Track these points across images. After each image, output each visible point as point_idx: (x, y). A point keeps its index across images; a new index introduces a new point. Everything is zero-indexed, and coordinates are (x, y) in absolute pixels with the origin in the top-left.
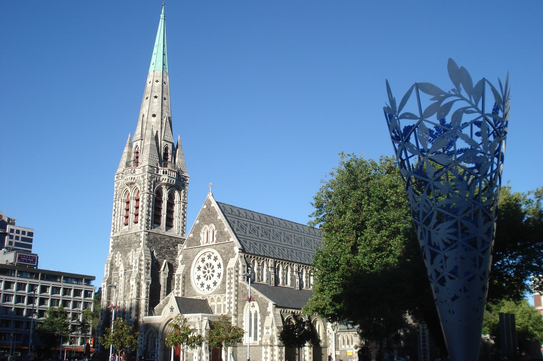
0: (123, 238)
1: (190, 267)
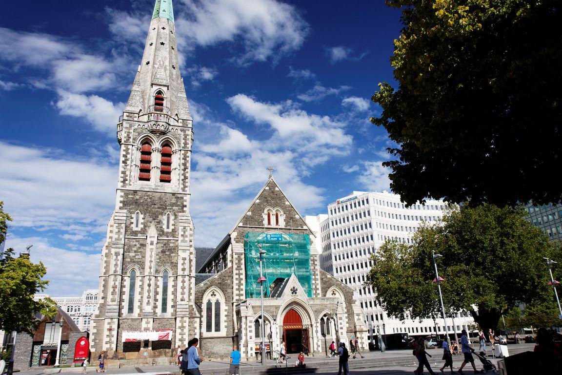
0: (148, 196)
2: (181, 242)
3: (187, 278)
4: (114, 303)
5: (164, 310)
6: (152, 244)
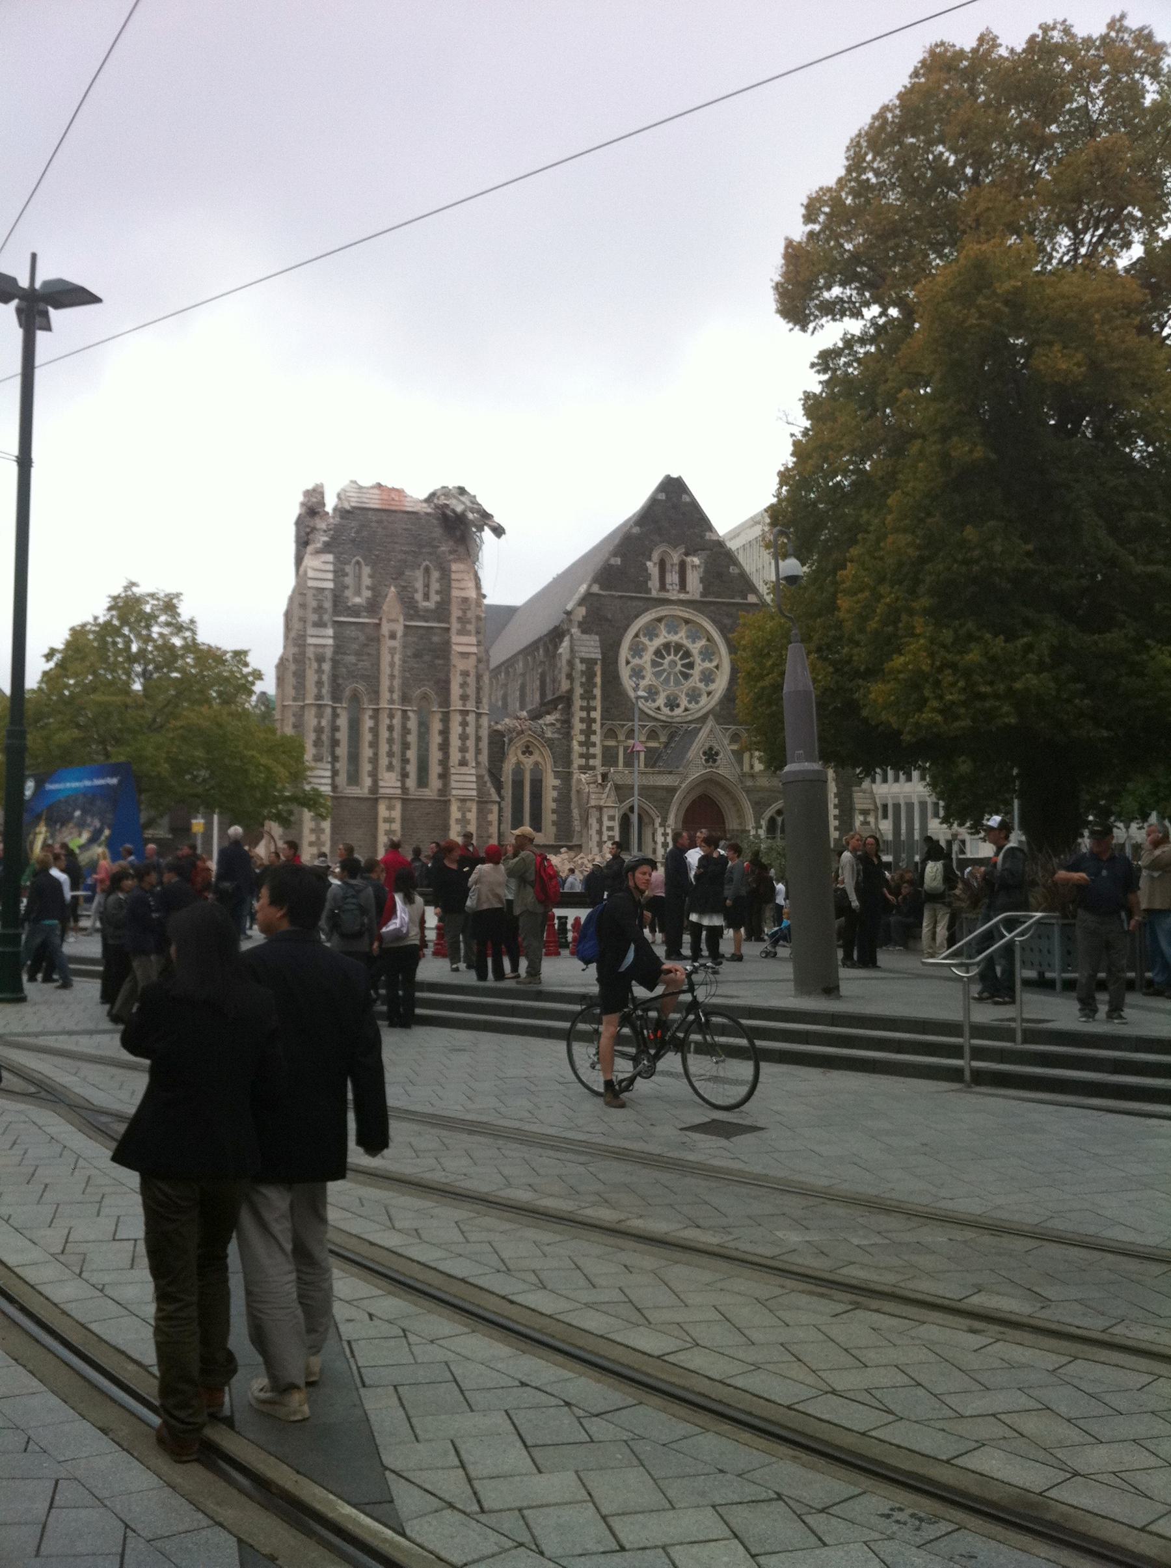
1: (618, 644)
3: (471, 718)
4: (319, 765)
5: (422, 782)
6: (393, 636)
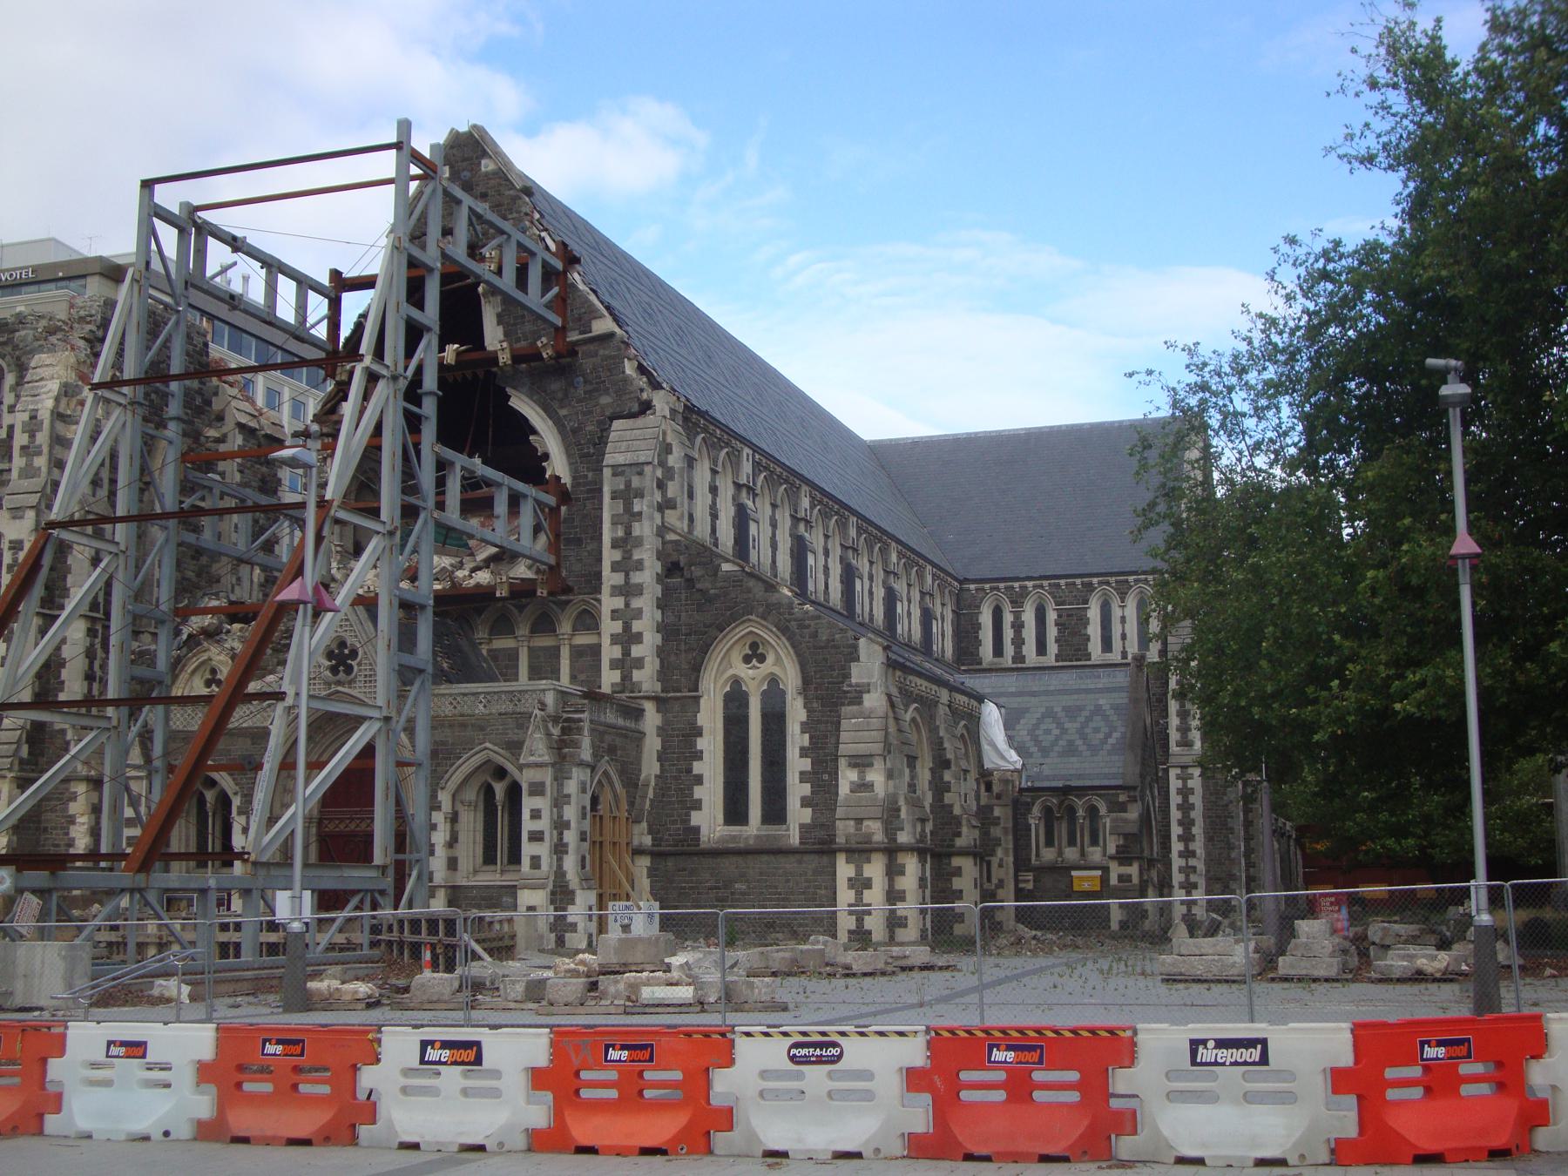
2: (20, 477)
